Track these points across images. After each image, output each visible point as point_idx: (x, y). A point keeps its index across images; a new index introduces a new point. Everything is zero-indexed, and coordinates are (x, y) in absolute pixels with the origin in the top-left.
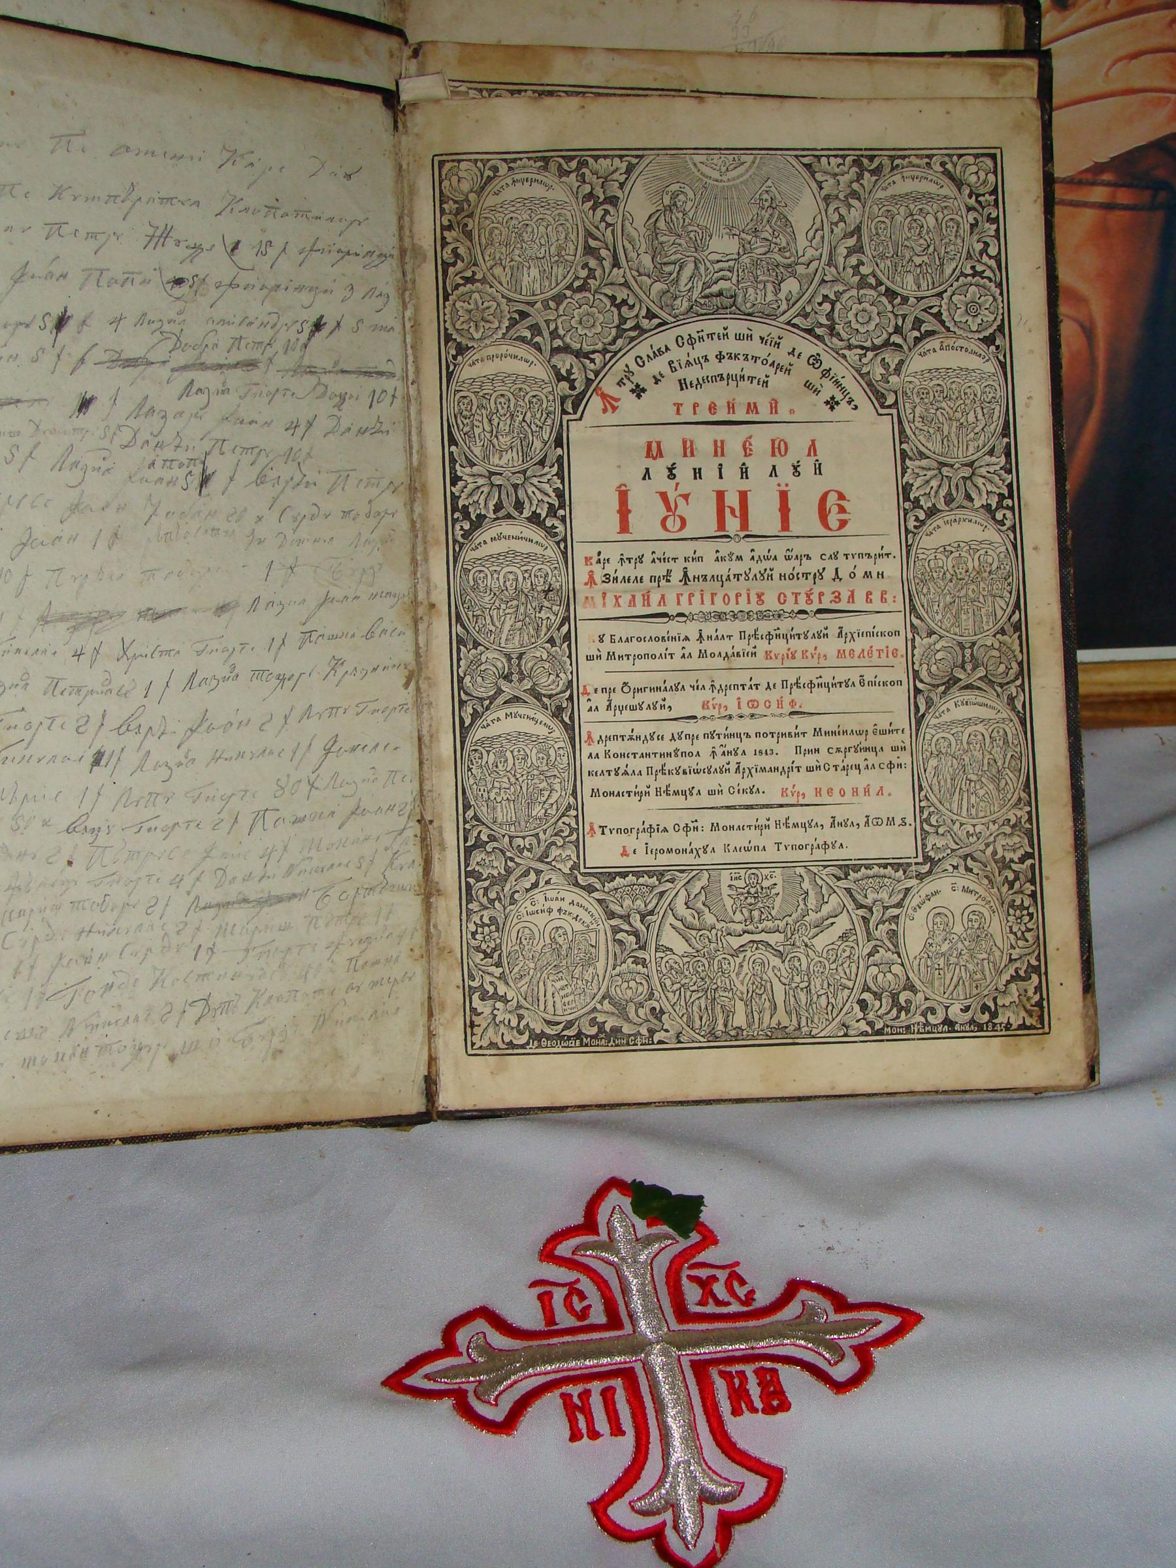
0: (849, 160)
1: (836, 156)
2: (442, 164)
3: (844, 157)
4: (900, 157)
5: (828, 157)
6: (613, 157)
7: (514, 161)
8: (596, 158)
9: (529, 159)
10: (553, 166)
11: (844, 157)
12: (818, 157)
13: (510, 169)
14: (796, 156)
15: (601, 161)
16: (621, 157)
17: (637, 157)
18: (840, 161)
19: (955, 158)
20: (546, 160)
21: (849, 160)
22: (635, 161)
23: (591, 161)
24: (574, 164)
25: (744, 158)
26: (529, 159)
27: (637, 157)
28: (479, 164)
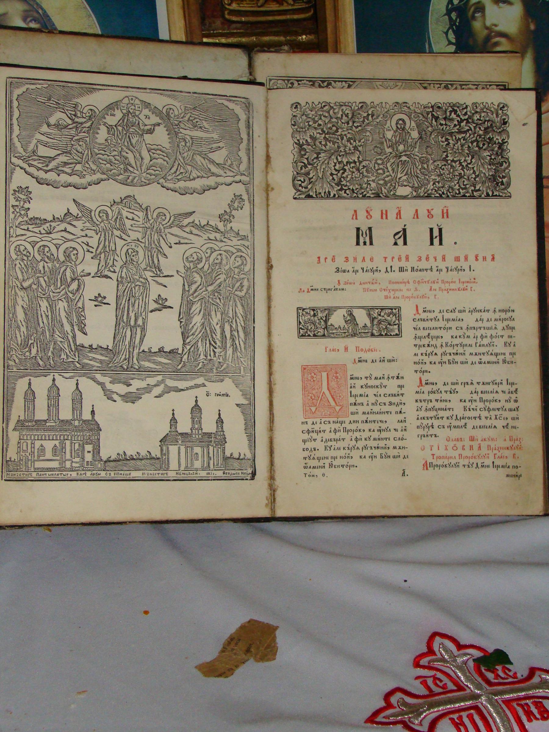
0: (443, 85)
1: (437, 84)
2: (270, 80)
3: (440, 84)
4: (464, 85)
5: (434, 84)
6: (342, 81)
7: (301, 81)
8: (335, 82)
9: (307, 80)
10: (317, 84)
11: (440, 84)
12: (430, 84)
13: (299, 84)
14: (420, 84)
15: (337, 83)
16: (346, 82)
17: (352, 82)
18: (438, 86)
19: (488, 86)
20: (314, 82)
21: (443, 85)
22: (351, 83)
23: (333, 83)
24: (325, 84)
25: (398, 84)
26: (307, 80)
27: (352, 82)
28: (286, 81)
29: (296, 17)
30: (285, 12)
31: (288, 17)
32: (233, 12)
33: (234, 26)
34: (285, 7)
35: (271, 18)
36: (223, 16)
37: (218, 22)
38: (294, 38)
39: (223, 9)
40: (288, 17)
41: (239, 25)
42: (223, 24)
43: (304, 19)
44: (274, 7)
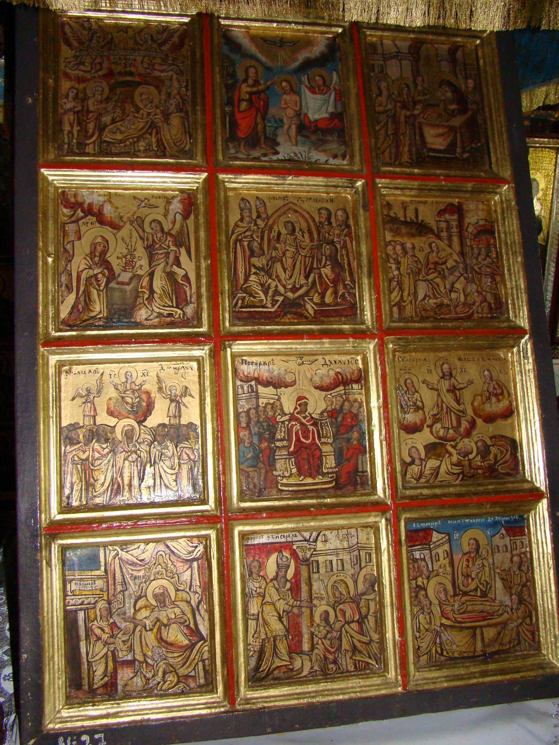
29: (324, 486)
30: (317, 484)
31: (319, 487)
32: (283, 485)
33: (284, 493)
34: (317, 481)
35: (307, 488)
36: (277, 487)
37: (274, 492)
38: (322, 500)
39: (277, 482)
40: (319, 487)
41: (287, 493)
42: (277, 492)
43: (329, 488)
44: (309, 480)
